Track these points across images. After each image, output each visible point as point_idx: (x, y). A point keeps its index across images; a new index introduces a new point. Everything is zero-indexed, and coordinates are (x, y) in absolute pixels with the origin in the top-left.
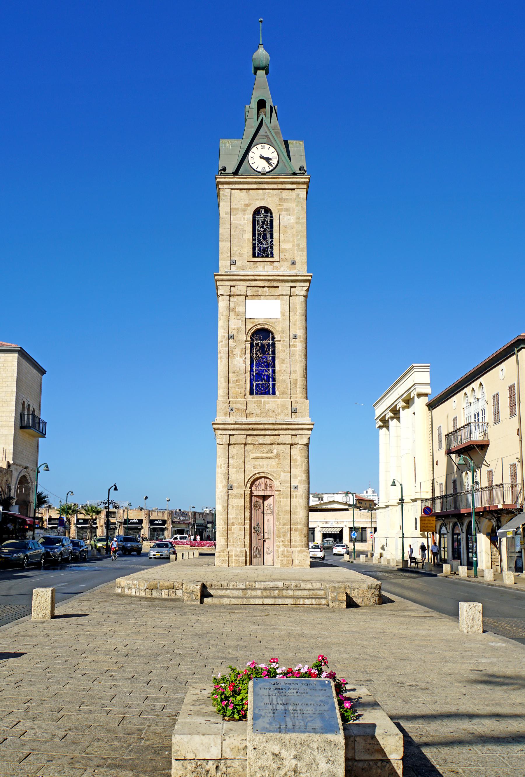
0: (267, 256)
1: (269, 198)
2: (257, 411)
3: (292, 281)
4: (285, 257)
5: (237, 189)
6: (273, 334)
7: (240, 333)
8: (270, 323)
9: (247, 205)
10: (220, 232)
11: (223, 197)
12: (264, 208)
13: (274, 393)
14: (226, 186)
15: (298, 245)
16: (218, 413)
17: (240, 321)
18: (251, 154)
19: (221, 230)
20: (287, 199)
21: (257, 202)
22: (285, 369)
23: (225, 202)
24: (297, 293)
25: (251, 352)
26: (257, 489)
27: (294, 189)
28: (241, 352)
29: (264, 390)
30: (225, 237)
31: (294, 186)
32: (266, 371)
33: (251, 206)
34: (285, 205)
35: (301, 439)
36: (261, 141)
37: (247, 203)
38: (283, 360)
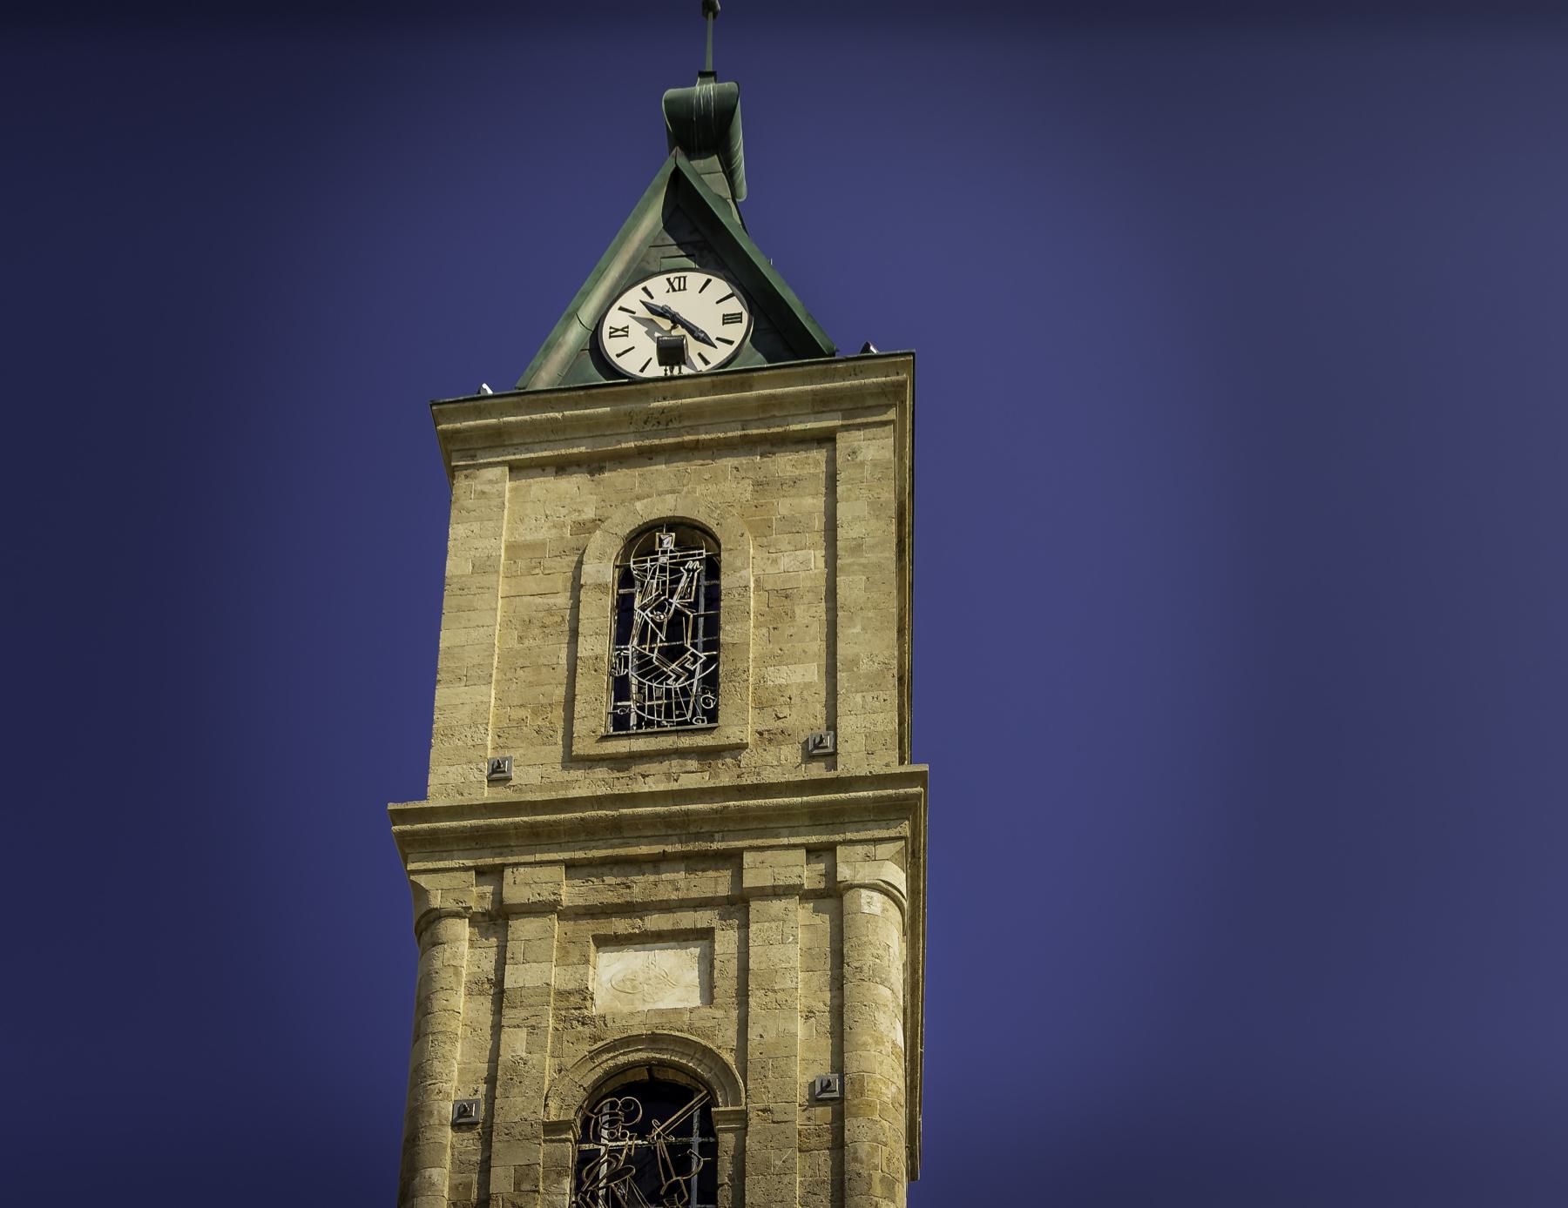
0: (684, 728)
11: (468, 503)
12: (672, 524)
15: (854, 662)
17: (523, 1033)
19: (447, 639)
21: (639, 505)
23: (478, 519)
24: (844, 873)
27: (826, 439)
28: (517, 1185)
34: (784, 506)
37: (589, 513)
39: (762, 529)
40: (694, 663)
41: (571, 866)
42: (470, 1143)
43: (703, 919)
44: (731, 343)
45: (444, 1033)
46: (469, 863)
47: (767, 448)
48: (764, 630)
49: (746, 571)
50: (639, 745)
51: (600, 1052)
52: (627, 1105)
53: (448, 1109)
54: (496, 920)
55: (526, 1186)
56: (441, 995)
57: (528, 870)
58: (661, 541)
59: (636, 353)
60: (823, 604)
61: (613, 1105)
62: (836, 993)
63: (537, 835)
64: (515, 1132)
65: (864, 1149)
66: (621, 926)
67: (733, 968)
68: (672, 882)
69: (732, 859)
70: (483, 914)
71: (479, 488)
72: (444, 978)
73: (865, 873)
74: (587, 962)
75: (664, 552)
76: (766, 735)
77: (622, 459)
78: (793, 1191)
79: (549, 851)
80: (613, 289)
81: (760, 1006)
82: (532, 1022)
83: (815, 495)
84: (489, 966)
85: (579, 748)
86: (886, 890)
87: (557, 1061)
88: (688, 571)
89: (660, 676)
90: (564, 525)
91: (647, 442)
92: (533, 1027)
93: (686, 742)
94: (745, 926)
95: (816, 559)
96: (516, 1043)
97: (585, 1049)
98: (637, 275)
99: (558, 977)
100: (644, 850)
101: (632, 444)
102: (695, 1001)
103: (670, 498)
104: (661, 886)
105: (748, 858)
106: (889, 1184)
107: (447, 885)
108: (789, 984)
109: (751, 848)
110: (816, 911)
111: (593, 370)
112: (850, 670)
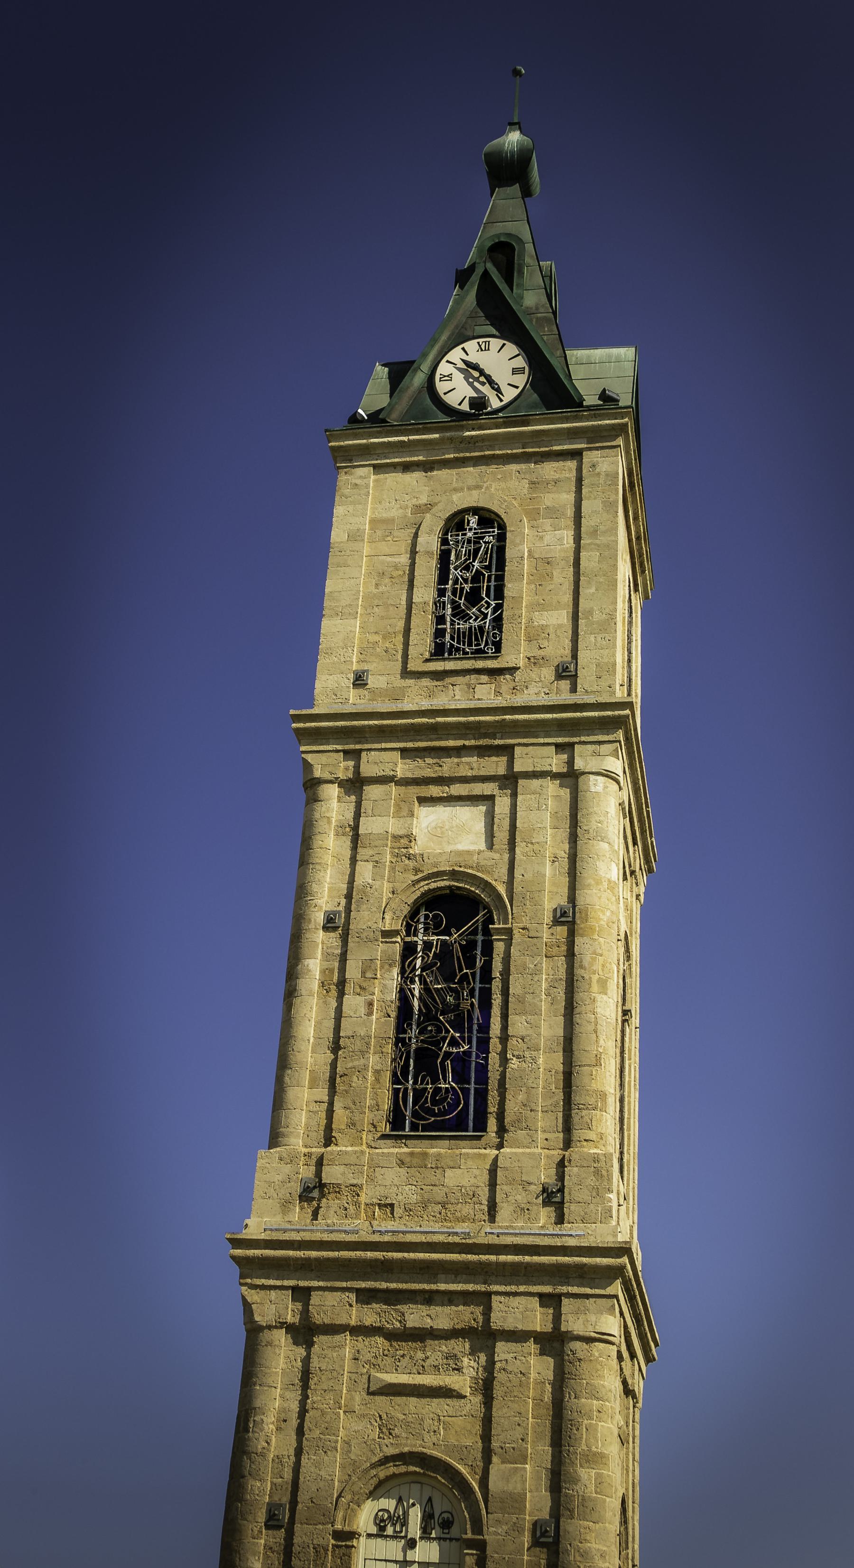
0: (480, 653)
2: (408, 1195)
3: (563, 727)
4: (541, 653)
5: (394, 467)
8: (478, 867)
9: (422, 509)
11: (347, 492)
12: (475, 511)
13: (481, 1126)
15: (590, 612)
16: (257, 1204)
17: (370, 866)
19: (330, 586)
21: (455, 497)
22: (524, 1033)
23: (352, 503)
25: (406, 974)
26: (390, 1531)
27: (577, 455)
28: (363, 973)
29: (442, 1113)
30: (343, 603)
32: (454, 1043)
33: (434, 510)
34: (548, 499)
35: (577, 1312)
36: (479, 330)
37: (423, 500)
38: (521, 1001)
39: (534, 515)
40: (487, 608)
41: (405, 753)
42: (333, 940)
43: (488, 788)
44: (517, 387)
45: (319, 864)
46: (339, 747)
47: (539, 458)
48: (533, 586)
49: (522, 546)
50: (450, 665)
51: (419, 881)
52: (435, 916)
53: (319, 918)
54: (355, 785)
55: (369, 975)
56: (318, 837)
57: (377, 753)
58: (469, 522)
59: (457, 391)
60: (572, 569)
61: (427, 917)
62: (572, 845)
63: (383, 731)
64: (363, 936)
65: (587, 960)
66: (435, 791)
67: (506, 823)
68: (468, 763)
69: (508, 751)
70: (347, 780)
71: (354, 481)
72: (321, 825)
73: (592, 764)
74: (413, 815)
75: (470, 529)
76: (532, 660)
78: (540, 986)
79: (391, 742)
80: (442, 347)
84: (350, 815)
85: (411, 666)
86: (608, 775)
87: (391, 885)
88: (485, 542)
89: (465, 617)
90: (407, 507)
91: (462, 455)
92: (377, 862)
93: (480, 664)
94: (514, 795)
95: (568, 536)
96: (365, 873)
98: (459, 339)
99: (392, 825)
100: (451, 743)
101: (452, 456)
102: (482, 846)
104: (461, 766)
105: (518, 751)
106: (603, 984)
108: (542, 839)
109: (519, 745)
110: (561, 786)
111: (428, 401)
112: (587, 618)
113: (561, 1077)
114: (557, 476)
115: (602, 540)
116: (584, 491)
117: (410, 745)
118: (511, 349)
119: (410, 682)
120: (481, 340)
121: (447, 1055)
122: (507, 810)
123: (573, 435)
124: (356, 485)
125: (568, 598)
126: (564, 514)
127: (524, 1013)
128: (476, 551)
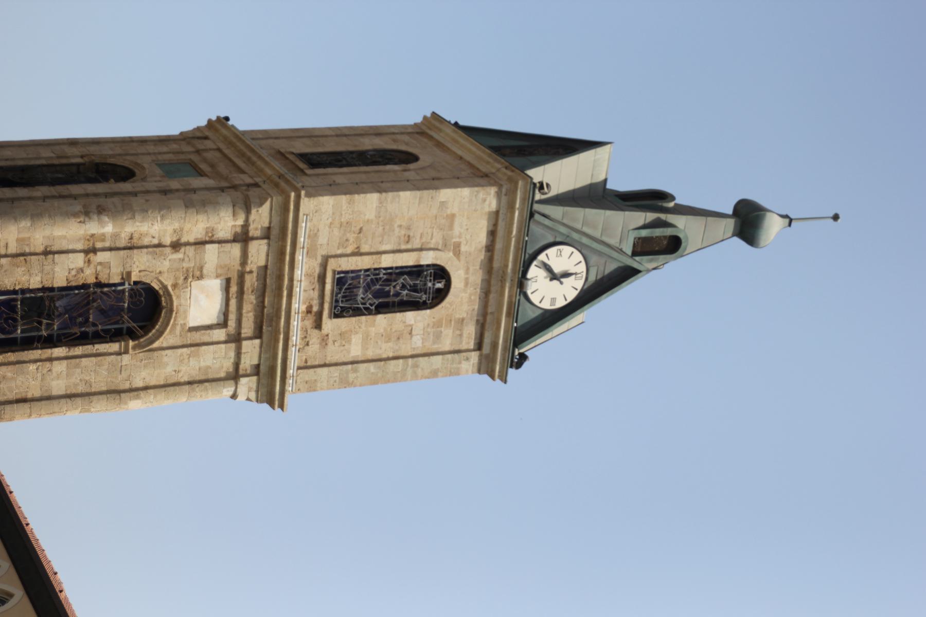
0: (337, 301)
1: (467, 295)
3: (272, 369)
6: (146, 329)
7: (150, 257)
8: (175, 325)
10: (402, 194)
14: (504, 199)
15: (355, 371)
18: (567, 250)
19: (406, 196)
20: (461, 335)
21: (462, 273)
24: (243, 381)
27: (479, 346)
28: (100, 264)
31: (486, 349)
33: (455, 258)
37: (463, 248)
38: (77, 366)
39: (438, 324)
41: (266, 267)
43: (232, 323)
50: (328, 287)
54: (243, 238)
56: (205, 218)
64: (128, 260)
66: (234, 289)
67: (206, 339)
69: (258, 333)
77: (490, 260)
81: (181, 355)
82: (186, 259)
83: (451, 344)
89: (368, 288)
93: (327, 306)
94: (226, 342)
97: (169, 284)
103: (462, 285)
105: (257, 341)
107: (261, 216)
113: (23, 395)
114: (465, 335)
115: (410, 371)
116: (449, 356)
117: (269, 272)
118: (572, 295)
119: (319, 260)
120: (584, 274)
121: (40, 323)
122: (215, 339)
123: (494, 346)
124: (484, 200)
125: (370, 354)
126: (434, 343)
127: (68, 367)
128: (416, 291)
